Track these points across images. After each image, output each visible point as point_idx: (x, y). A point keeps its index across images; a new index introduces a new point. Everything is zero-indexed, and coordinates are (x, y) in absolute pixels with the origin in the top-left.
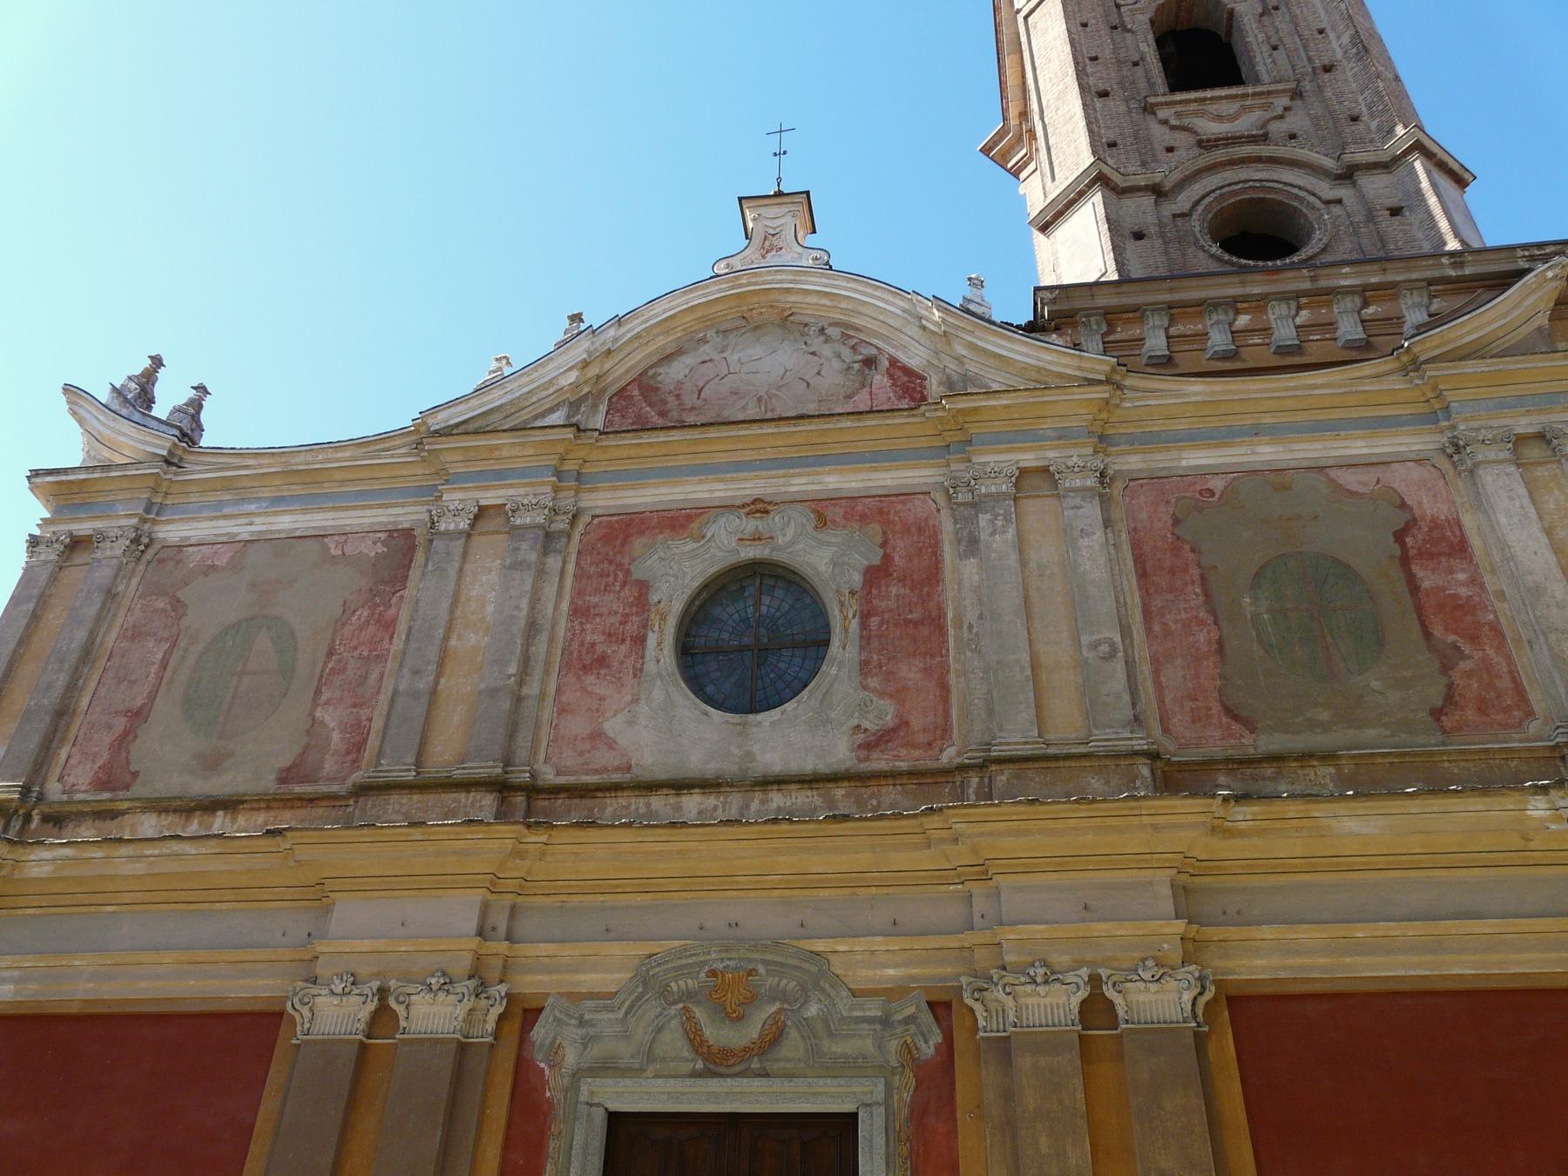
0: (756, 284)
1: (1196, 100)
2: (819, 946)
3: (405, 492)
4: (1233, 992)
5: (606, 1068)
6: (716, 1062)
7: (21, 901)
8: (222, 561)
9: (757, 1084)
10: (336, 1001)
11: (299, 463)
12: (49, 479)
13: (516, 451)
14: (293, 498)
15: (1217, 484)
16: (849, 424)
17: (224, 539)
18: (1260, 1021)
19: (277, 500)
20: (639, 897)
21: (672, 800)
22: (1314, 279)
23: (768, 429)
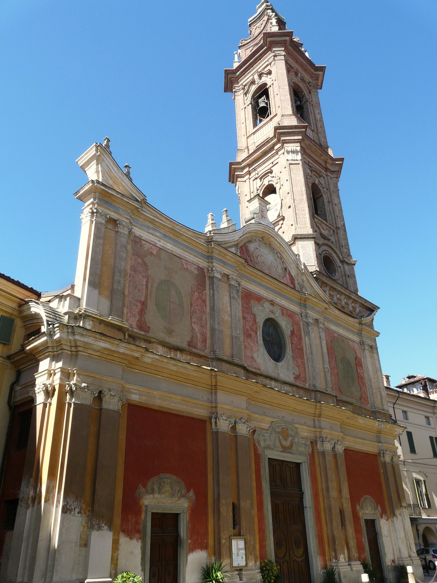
0: (268, 231)
1: (321, 221)
2: (297, 426)
3: (198, 253)
4: (131, 402)
5: (268, 447)
6: (285, 449)
7: (135, 367)
8: (155, 252)
9: (290, 455)
10: (224, 421)
11: (177, 228)
12: (102, 187)
13: (230, 258)
14: (170, 238)
15: (336, 335)
16: (289, 289)
17: (153, 243)
18: (138, 413)
19: (165, 236)
20: (269, 406)
21: (270, 381)
22: (350, 294)
23: (276, 282)
